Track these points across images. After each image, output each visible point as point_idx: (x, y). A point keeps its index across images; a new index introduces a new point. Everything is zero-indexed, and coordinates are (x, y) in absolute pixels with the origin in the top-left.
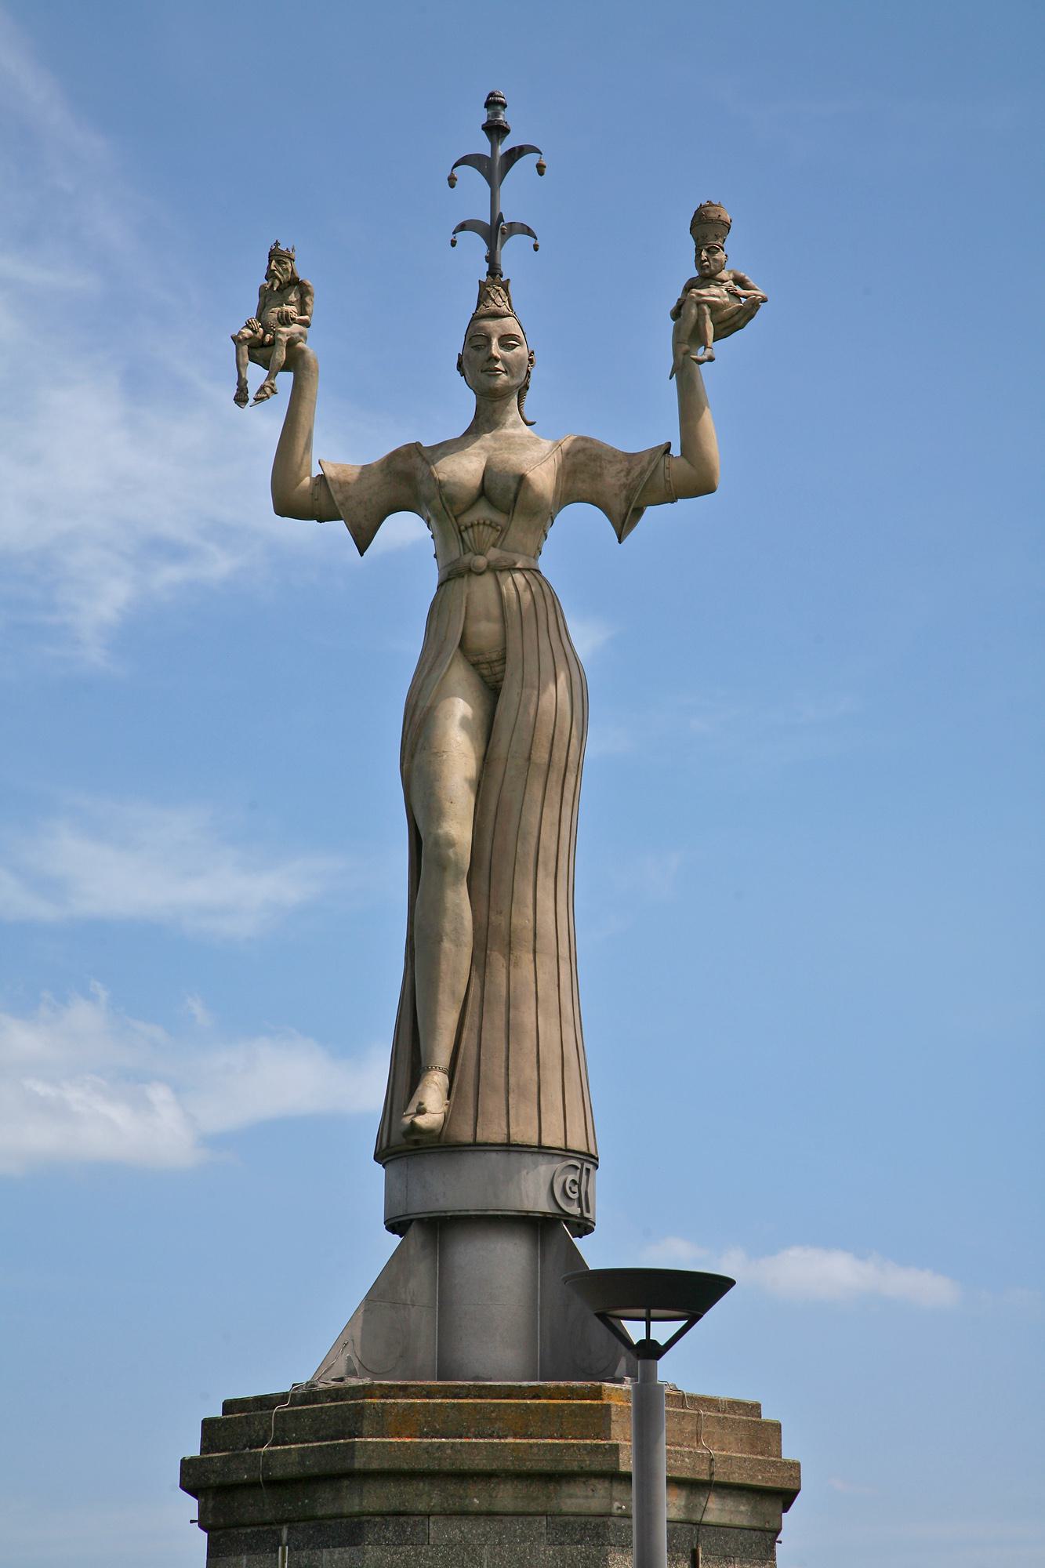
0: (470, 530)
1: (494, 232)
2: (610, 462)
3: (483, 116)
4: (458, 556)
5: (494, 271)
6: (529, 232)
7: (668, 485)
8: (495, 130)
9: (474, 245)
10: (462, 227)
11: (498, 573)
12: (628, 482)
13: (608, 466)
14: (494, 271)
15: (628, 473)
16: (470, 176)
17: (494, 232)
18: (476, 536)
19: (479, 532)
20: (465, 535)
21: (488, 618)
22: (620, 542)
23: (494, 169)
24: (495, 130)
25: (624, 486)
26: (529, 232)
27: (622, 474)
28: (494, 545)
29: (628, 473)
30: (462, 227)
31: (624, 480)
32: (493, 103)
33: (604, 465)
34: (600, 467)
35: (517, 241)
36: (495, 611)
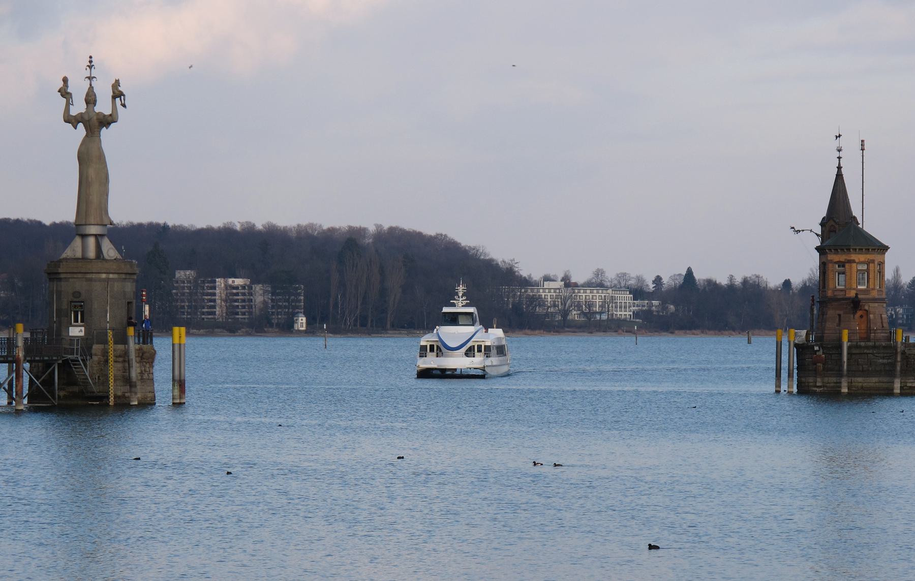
1: (90, 78)
3: (89, 59)
5: (91, 85)
6: (95, 78)
8: (91, 62)
9: (88, 81)
10: (86, 78)
14: (91, 85)
16: (88, 68)
17: (90, 78)
23: (90, 67)
24: (91, 62)
26: (95, 78)
30: (86, 78)
32: (91, 57)
35: (94, 79)
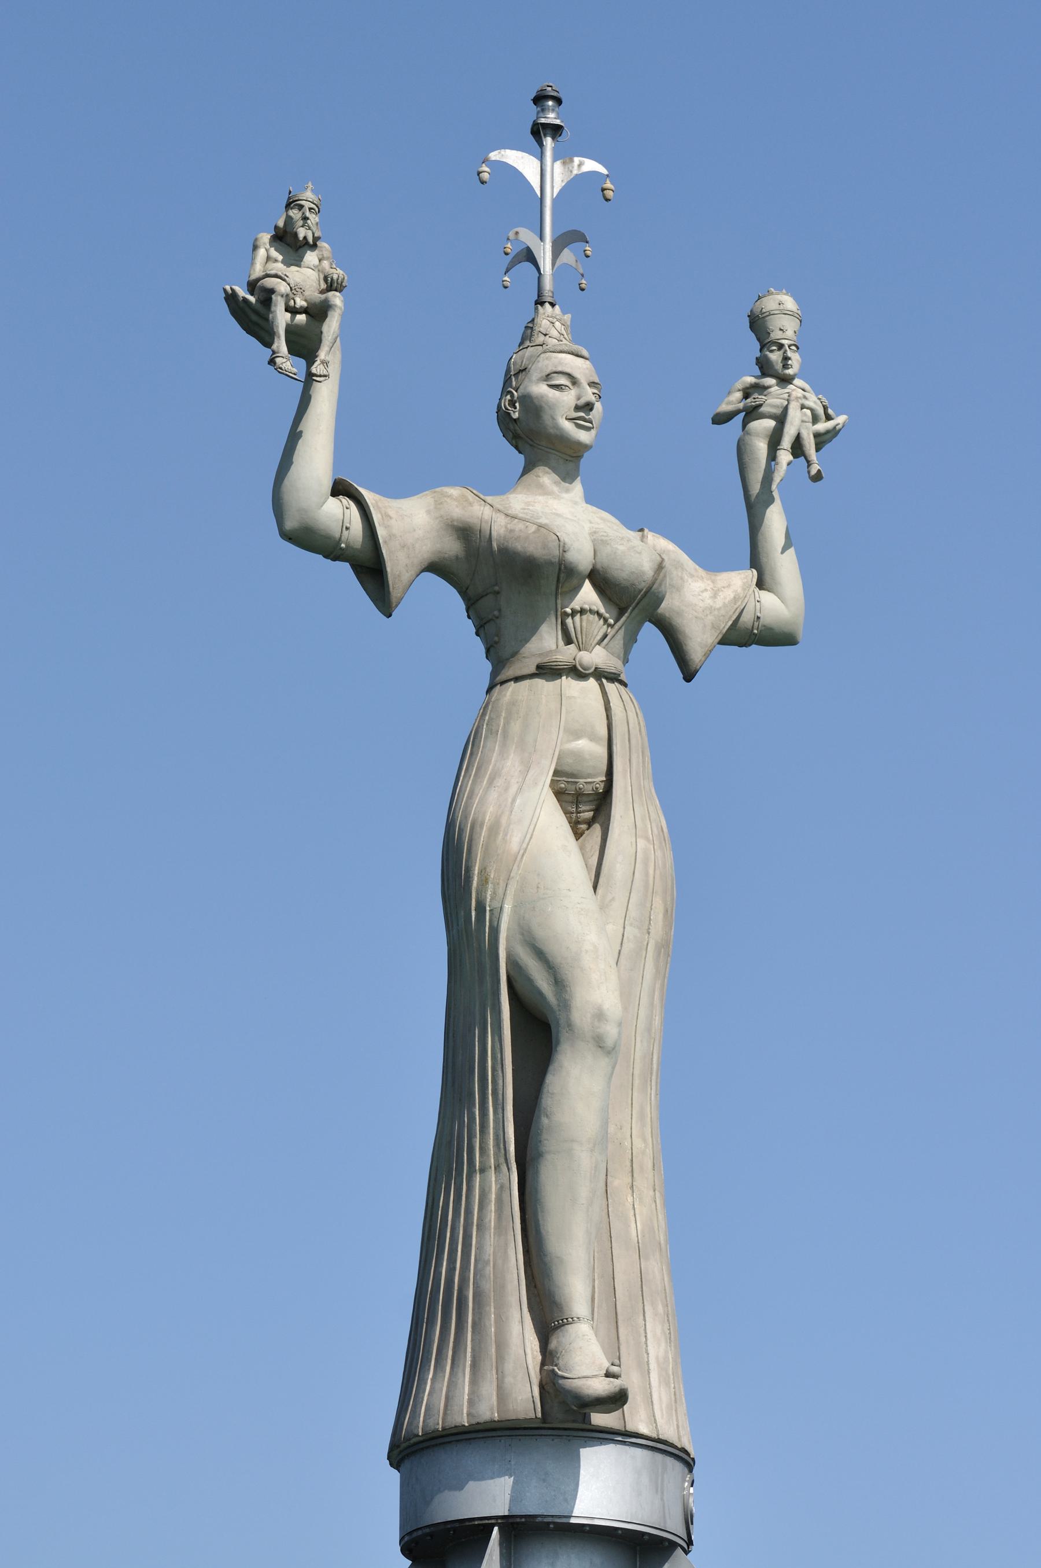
0: (577, 618)
2: (692, 576)
4: (554, 647)
7: (756, 624)
11: (604, 681)
12: (718, 606)
13: (690, 580)
15: (715, 596)
18: (584, 624)
19: (588, 620)
20: (569, 621)
21: (593, 738)
22: (689, 676)
25: (711, 609)
27: (707, 595)
28: (599, 643)
29: (715, 596)
31: (709, 602)
33: (686, 577)
34: (682, 578)
36: (604, 732)
